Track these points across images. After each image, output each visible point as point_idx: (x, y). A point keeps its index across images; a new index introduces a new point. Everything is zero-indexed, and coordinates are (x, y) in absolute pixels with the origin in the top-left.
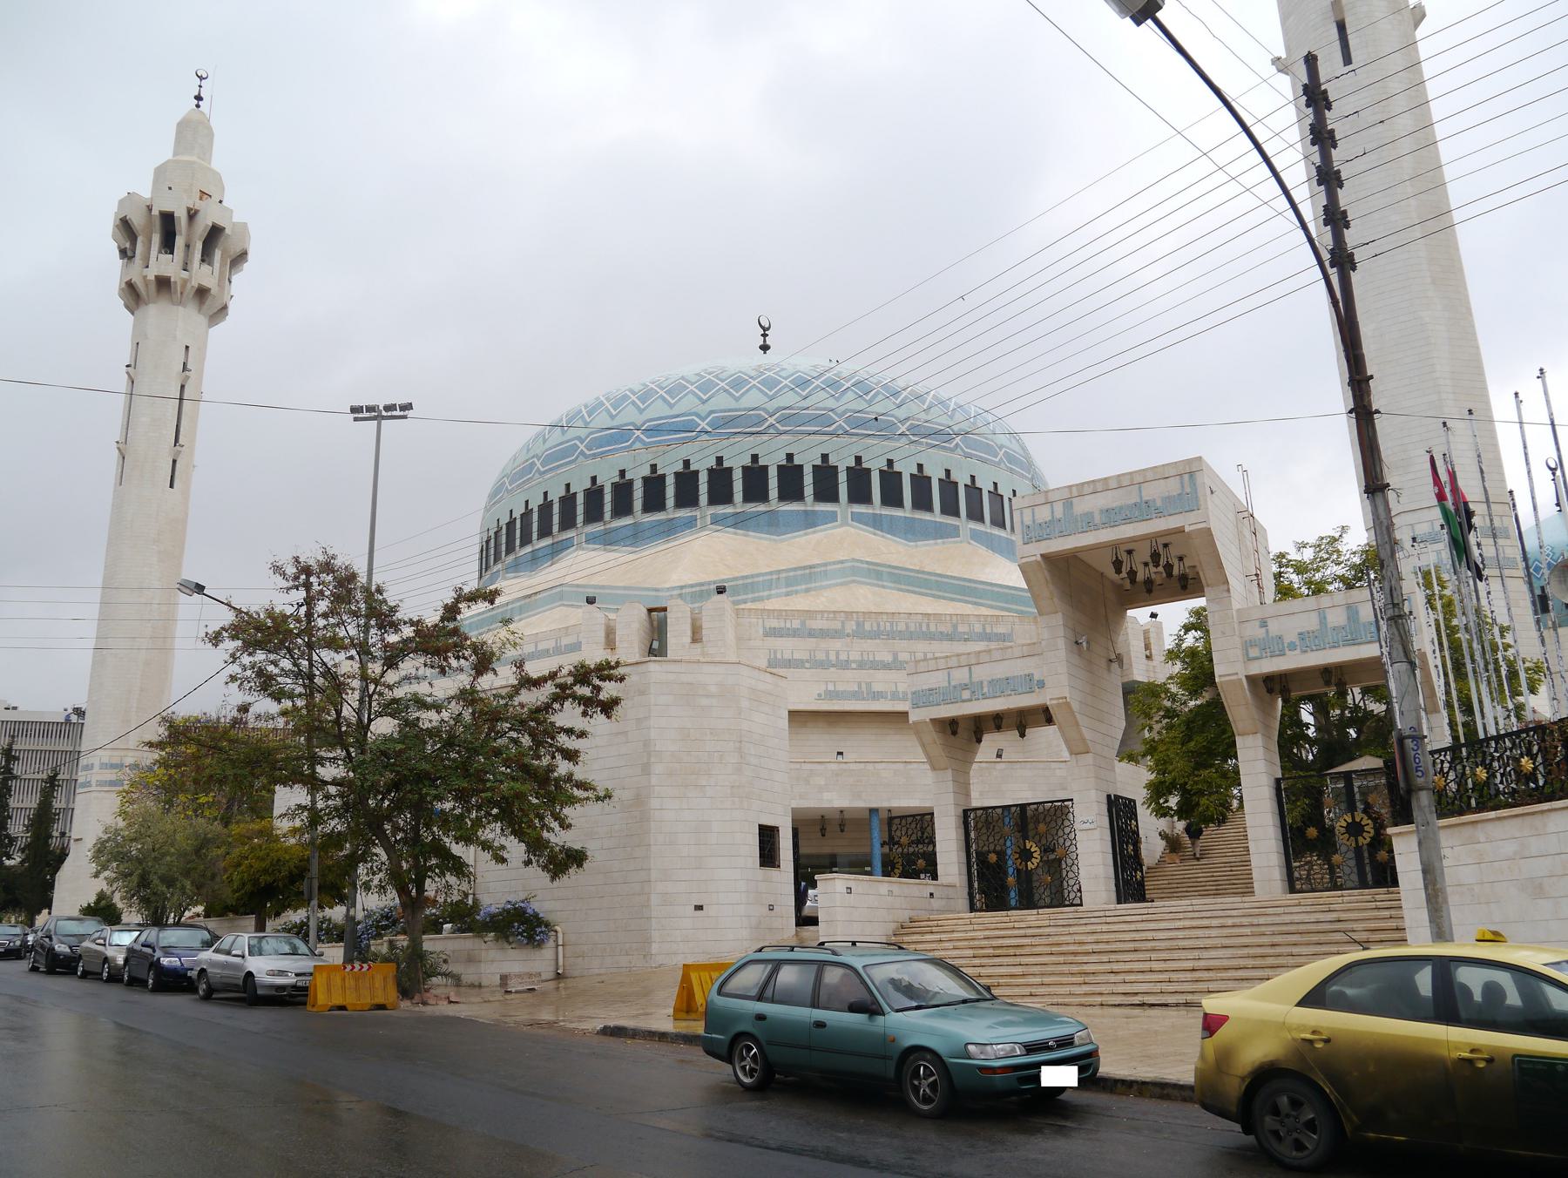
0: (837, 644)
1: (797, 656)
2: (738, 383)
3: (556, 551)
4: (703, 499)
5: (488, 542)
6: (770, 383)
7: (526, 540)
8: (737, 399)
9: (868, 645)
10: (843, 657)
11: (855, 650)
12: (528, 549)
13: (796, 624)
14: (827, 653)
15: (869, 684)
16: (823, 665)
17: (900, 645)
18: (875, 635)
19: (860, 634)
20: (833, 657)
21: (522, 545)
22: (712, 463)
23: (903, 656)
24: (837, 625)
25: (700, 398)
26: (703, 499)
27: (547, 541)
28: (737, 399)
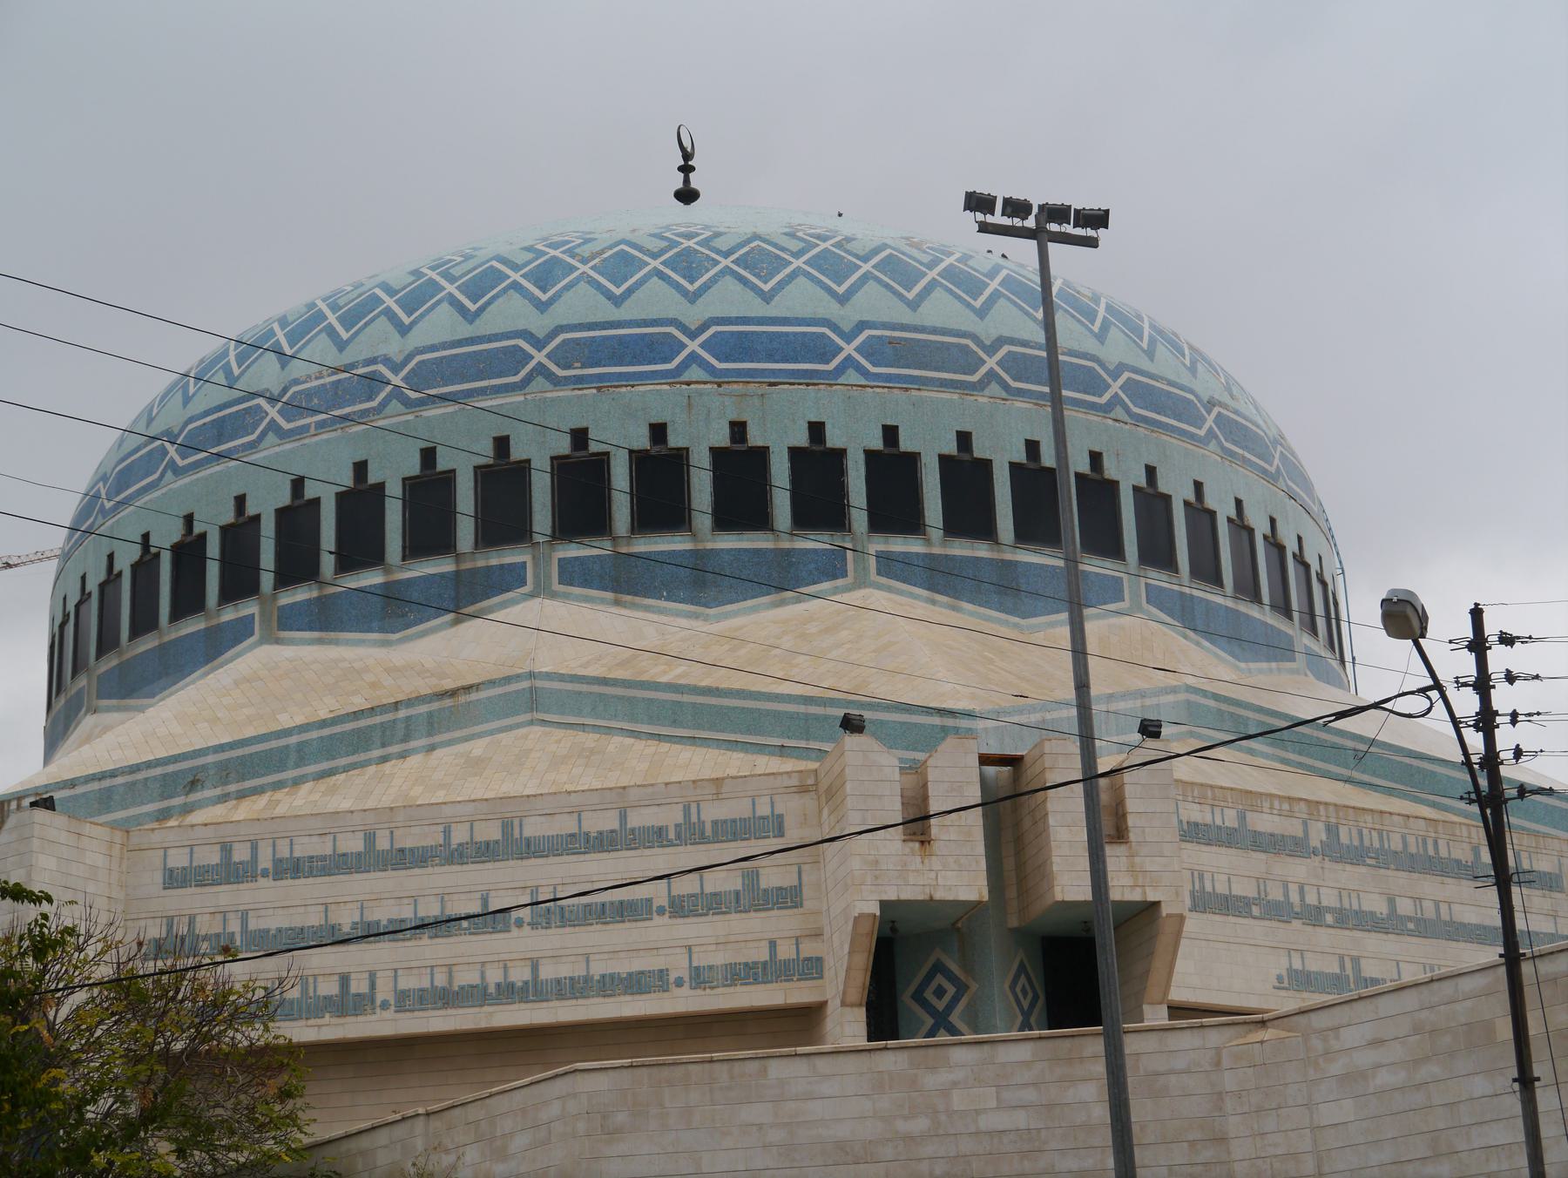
0: (1297, 870)
1: (1237, 890)
2: (621, 264)
3: (215, 646)
4: (859, 518)
5: (62, 626)
6: (688, 264)
7: (144, 622)
8: (767, 298)
9: (1349, 875)
10: (1311, 899)
11: (1333, 884)
12: (148, 643)
13: (1230, 819)
14: (1285, 885)
15: (1356, 961)
16: (1278, 912)
17: (1399, 880)
18: (1356, 856)
19: (1335, 852)
20: (1295, 897)
21: (135, 633)
22: (485, 452)
23: (1405, 907)
24: (1293, 828)
25: (609, 296)
26: (859, 518)
27: (193, 626)
28: (767, 298)
